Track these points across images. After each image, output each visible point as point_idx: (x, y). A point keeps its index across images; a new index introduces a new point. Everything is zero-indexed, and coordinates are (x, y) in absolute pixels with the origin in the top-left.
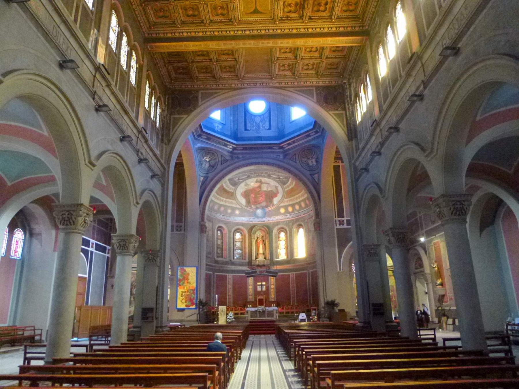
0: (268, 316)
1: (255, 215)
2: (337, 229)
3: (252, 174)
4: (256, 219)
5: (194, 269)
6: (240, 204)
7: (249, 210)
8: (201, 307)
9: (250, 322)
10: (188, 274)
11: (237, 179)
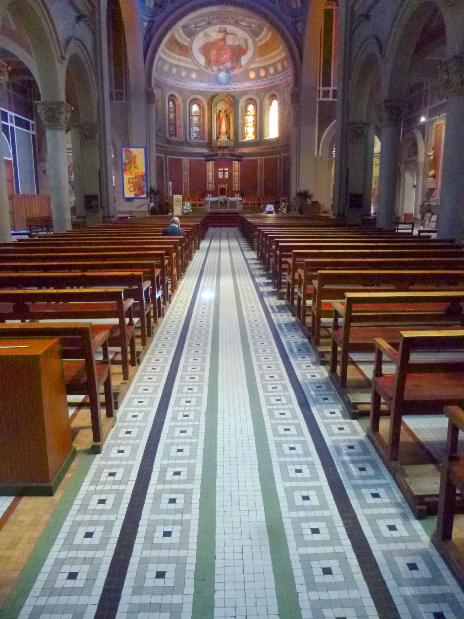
0: (230, 208)
1: (217, 81)
2: (320, 102)
3: (214, 19)
4: (218, 86)
5: (142, 150)
7: (210, 72)
8: (152, 196)
9: (210, 213)
10: (135, 157)
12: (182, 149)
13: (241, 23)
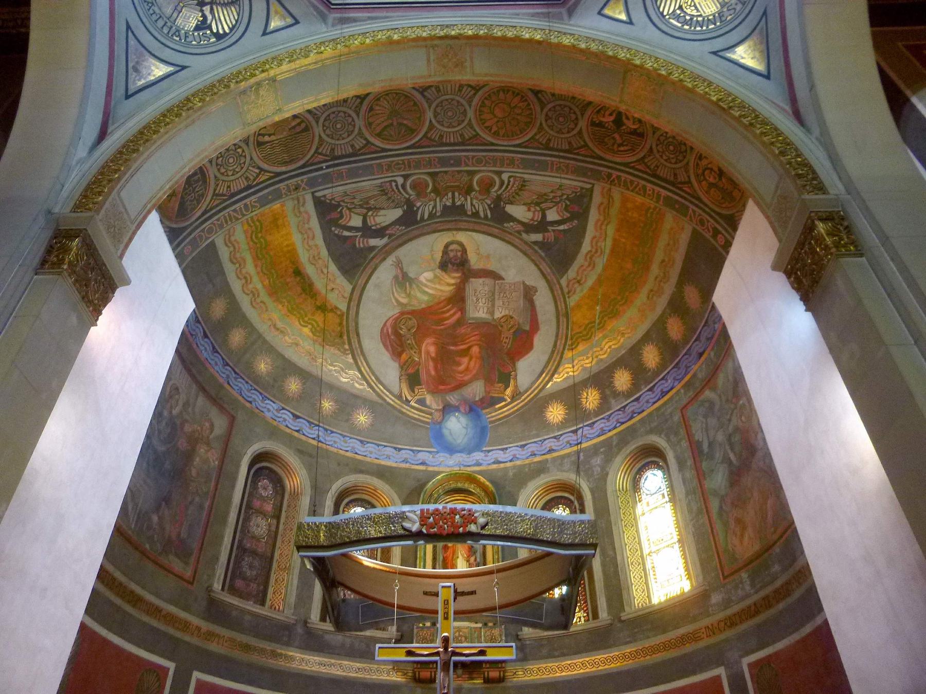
4: (442, 457)
6: (371, 376)
7: (415, 414)
11: (356, 221)
12: (274, 655)
13: (511, 209)
